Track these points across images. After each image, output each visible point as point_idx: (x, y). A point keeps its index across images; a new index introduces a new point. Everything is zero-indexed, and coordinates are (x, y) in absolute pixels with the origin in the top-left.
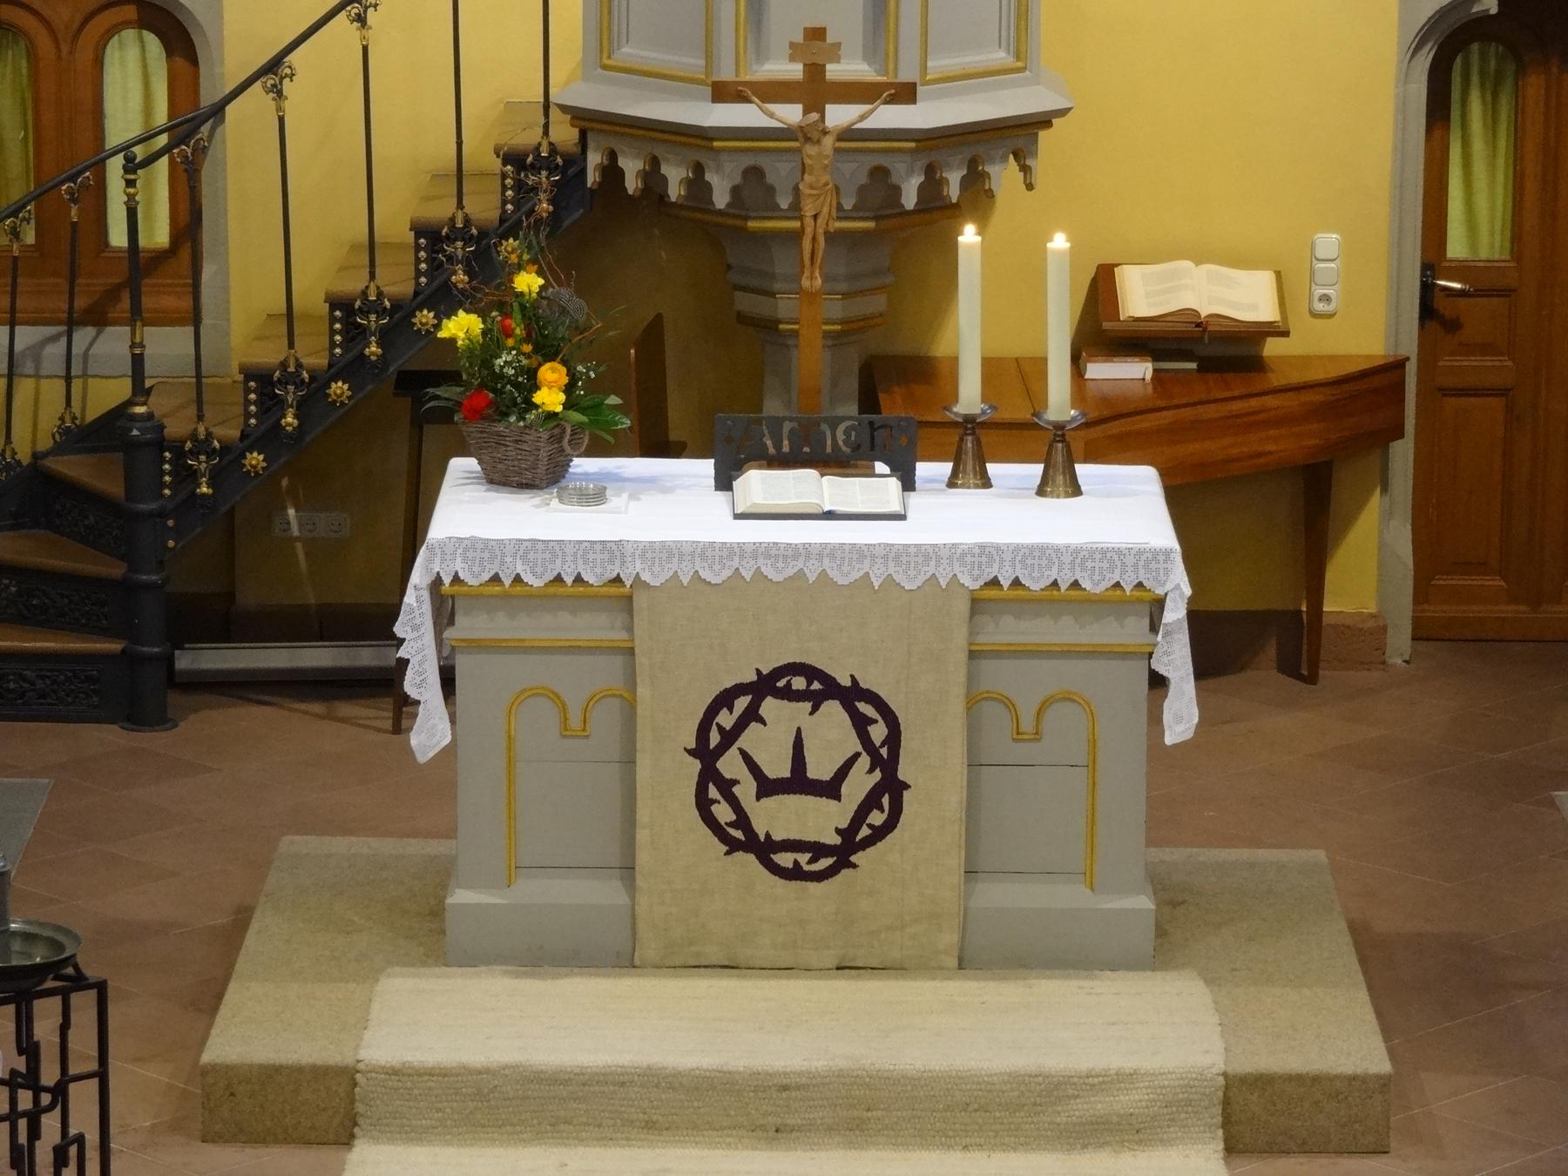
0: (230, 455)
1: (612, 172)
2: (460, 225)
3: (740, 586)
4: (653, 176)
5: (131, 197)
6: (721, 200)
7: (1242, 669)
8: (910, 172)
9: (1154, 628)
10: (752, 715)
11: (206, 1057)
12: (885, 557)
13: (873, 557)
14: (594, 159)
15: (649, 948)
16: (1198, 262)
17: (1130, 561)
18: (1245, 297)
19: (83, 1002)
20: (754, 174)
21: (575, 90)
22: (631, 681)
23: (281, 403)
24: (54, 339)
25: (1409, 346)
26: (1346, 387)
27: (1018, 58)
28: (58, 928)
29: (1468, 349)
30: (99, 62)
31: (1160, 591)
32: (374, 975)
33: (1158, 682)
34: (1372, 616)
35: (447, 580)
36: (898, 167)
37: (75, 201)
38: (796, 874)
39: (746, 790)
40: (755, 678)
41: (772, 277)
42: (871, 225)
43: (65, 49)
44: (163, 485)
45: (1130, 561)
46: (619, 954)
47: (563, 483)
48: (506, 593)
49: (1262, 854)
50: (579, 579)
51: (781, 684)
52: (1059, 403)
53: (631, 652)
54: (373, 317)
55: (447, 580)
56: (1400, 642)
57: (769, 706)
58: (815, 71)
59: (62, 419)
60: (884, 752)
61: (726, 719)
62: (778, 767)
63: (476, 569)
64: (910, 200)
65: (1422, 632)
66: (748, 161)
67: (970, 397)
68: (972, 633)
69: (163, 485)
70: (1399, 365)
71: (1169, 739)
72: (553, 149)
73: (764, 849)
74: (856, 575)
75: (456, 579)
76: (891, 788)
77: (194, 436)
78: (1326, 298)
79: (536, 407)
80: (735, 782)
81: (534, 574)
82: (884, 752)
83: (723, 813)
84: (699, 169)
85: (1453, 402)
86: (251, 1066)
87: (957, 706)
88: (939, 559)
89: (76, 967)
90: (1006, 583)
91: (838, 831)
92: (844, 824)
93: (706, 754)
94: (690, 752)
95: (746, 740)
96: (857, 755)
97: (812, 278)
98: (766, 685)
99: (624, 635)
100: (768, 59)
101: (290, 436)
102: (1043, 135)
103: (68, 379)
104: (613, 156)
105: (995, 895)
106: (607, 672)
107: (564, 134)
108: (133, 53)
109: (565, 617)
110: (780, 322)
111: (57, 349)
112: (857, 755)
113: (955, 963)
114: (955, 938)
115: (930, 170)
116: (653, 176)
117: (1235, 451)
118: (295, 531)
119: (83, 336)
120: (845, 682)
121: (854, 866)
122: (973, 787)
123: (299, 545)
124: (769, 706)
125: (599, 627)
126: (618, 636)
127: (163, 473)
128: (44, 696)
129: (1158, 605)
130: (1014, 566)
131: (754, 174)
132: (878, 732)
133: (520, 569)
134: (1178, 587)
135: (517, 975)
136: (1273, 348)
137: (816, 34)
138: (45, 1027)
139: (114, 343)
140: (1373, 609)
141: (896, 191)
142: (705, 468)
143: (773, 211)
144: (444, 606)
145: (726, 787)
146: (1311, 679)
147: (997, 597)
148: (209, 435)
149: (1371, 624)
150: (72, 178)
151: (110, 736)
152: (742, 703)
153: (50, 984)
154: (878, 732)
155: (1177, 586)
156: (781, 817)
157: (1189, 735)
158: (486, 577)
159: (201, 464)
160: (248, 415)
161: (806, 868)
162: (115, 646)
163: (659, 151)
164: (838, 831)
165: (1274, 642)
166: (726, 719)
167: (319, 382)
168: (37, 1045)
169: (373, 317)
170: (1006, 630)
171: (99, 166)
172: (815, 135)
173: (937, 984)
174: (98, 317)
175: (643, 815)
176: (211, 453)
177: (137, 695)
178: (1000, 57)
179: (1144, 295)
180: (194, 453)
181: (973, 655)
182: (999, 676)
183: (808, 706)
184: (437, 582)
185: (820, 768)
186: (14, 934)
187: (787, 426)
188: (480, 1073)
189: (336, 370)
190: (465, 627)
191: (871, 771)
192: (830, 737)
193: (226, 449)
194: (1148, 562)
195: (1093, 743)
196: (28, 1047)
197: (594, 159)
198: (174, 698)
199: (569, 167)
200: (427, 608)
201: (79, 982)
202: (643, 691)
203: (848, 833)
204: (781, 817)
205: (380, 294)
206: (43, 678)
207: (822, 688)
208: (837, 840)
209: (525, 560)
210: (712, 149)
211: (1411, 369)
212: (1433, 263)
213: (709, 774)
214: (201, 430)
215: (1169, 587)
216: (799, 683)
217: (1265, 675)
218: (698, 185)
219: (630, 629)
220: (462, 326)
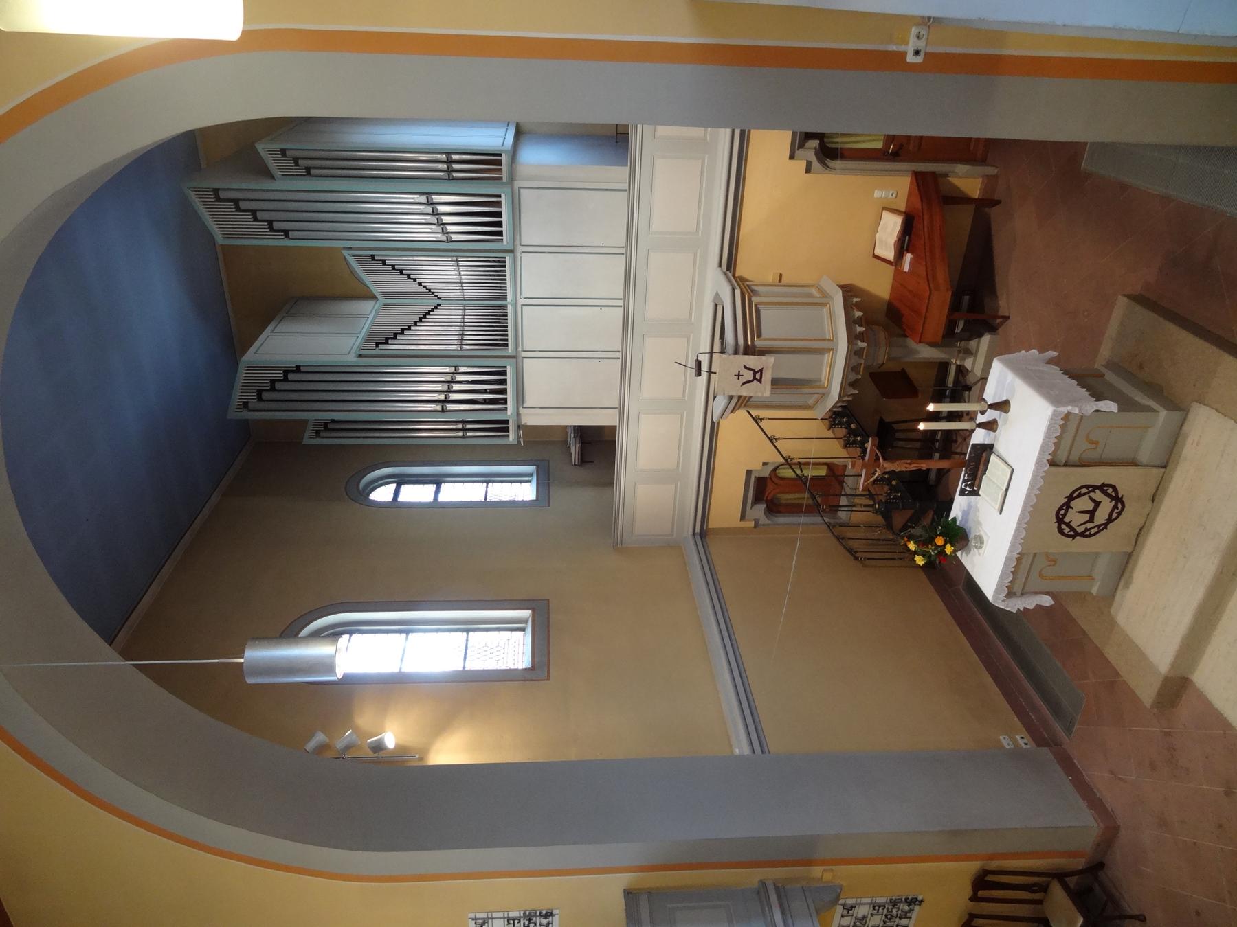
10: (1068, 525)
11: (1148, 706)
18: (891, 226)
36: (856, 348)
39: (1089, 525)
47: (971, 536)
56: (991, 171)
61: (1067, 530)
73: (1110, 520)
98: (1060, 521)
132: (1084, 491)
144: (1011, 594)
145: (1087, 530)
154: (1084, 491)
156: (1101, 516)
174: (841, 483)
185: (1091, 506)
203: (1112, 498)
204: (1101, 516)
207: (1067, 506)
213: (1082, 535)
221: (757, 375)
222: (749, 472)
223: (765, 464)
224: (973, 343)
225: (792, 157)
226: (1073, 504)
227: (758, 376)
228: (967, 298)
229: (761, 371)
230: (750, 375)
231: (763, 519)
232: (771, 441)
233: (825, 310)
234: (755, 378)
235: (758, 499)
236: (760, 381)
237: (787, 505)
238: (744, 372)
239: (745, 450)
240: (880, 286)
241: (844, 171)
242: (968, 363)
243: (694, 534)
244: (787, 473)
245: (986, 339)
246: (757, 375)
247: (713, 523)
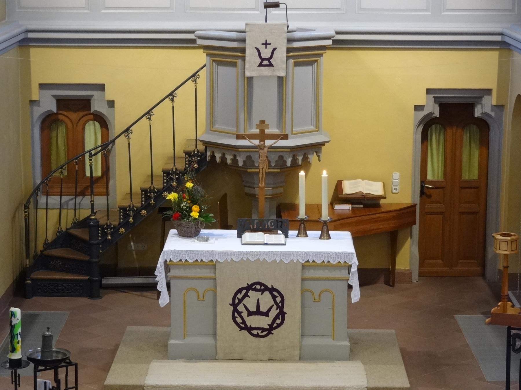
0: (116, 229)
1: (213, 157)
3: (243, 262)
4: (223, 158)
5: (91, 163)
6: (241, 164)
7: (375, 283)
8: (289, 157)
9: (349, 273)
10: (246, 295)
11: (106, 383)
12: (280, 255)
13: (277, 255)
14: (209, 154)
15: (220, 355)
17: (343, 256)
18: (375, 189)
19: (71, 369)
20: (249, 158)
21: (203, 136)
22: (215, 287)
23: (129, 216)
24: (72, 199)
25: (417, 201)
26: (401, 211)
27: (316, 128)
28: (66, 350)
29: (432, 202)
30: (83, 129)
31: (350, 264)
32: (149, 362)
33: (350, 287)
34: (408, 270)
35: (168, 261)
36: (285, 156)
37: (77, 164)
38: (257, 336)
39: (245, 314)
40: (247, 285)
41: (254, 183)
42: (279, 170)
43: (75, 126)
44: (99, 237)
45: (343, 256)
46: (212, 356)
47: (199, 236)
48: (183, 264)
49: (378, 331)
50: (202, 260)
51: (254, 287)
52: (325, 215)
53: (215, 279)
54: (152, 194)
55: (168, 261)
56: (415, 276)
57: (251, 293)
58: (262, 131)
59: (73, 220)
60: (280, 304)
61: (240, 296)
62: (253, 309)
63: (176, 258)
64: (289, 164)
65: (421, 274)
66: (248, 154)
67: (302, 214)
68: (302, 274)
69: (99, 237)
70: (414, 206)
71: (353, 302)
72: (198, 151)
73: (249, 329)
74: (273, 259)
75: (171, 261)
76: (282, 314)
77: (107, 224)
78: (396, 189)
79: (191, 216)
80: (242, 312)
81: (191, 259)
82: (280, 304)
83: (239, 320)
84: (235, 156)
85: (429, 216)
86: (117, 385)
87: (299, 293)
88: (294, 255)
89: (69, 360)
90: (311, 261)
91: (268, 325)
92: (270, 323)
93: (234, 305)
94: (230, 305)
95: (244, 302)
96: (273, 305)
97: (262, 184)
98: (249, 288)
99: (214, 275)
101: (131, 224)
102: (323, 147)
103: (75, 209)
104: (213, 153)
105: (309, 341)
106: (209, 284)
107: (201, 147)
108: (92, 127)
109: (198, 270)
111: (73, 202)
112: (273, 305)
113: (298, 358)
114: (298, 352)
115: (294, 156)
116: (223, 158)
117: (372, 228)
118: (133, 249)
119: (79, 199)
120: (270, 287)
121: (272, 334)
122: (303, 313)
123: (134, 252)
124: (251, 293)
125: (206, 273)
126: (212, 275)
127: (99, 233)
128: (68, 290)
129: (351, 266)
130: (313, 257)
131: (249, 158)
132: (278, 299)
133: (187, 258)
134: (355, 262)
135: (186, 362)
136: (382, 201)
137: (263, 122)
138: (62, 376)
139: (86, 201)
140: (409, 268)
141: (285, 162)
142: (235, 232)
143: (253, 166)
144: (168, 267)
145: (240, 313)
146: (393, 286)
147: (308, 265)
148: (110, 224)
149: (408, 272)
150: (76, 159)
151: (84, 301)
152: (244, 292)
153: (63, 364)
154: (278, 299)
155: (355, 262)
156: (254, 321)
157: (358, 300)
158: (178, 260)
159: (109, 231)
160: (120, 219)
161: (260, 334)
162: (86, 278)
163: (225, 151)
164: (268, 325)
165: (383, 277)
166: (240, 296)
167: (139, 210)
168: (59, 380)
169: (152, 194)
170: (311, 273)
171: (83, 156)
172: (262, 148)
173: (294, 364)
175: (218, 321)
176: (111, 228)
177: (92, 290)
178: (312, 128)
179: (349, 188)
180: (107, 229)
181: (303, 280)
182: (309, 285)
183: (261, 293)
184: (166, 261)
185: (263, 309)
186: (54, 351)
187: (256, 221)
188: (176, 387)
189: (143, 207)
190: (173, 272)
191: (277, 309)
192: (266, 301)
193: (115, 227)
194: (347, 256)
195: (334, 302)
196: (57, 380)
197: (209, 154)
198: (101, 291)
199: (203, 155)
200: (163, 268)
201: (70, 364)
202: (218, 289)
203: (271, 325)
204: (254, 321)
205: (154, 188)
206: (68, 286)
207: (264, 288)
208: (268, 327)
209: (188, 255)
211: (418, 207)
212: (423, 181)
213: (235, 310)
214: (108, 222)
215: (353, 262)
216: (258, 287)
217: (381, 285)
218: (235, 160)
219: (215, 273)
220: (172, 196)
221: (266, 62)
222: (101, 87)
223: (111, 104)
225: (429, 91)
226: (267, 293)
229: (271, 65)
230: (266, 54)
231: (38, 112)
232: (171, 94)
233: (312, 128)
234: (263, 59)
235: (63, 103)
236: (260, 65)
237: (49, 139)
238: (270, 49)
239: (130, 82)
241: (415, 141)
243: (28, 31)
244: (92, 135)
246: (266, 62)
247: (38, 55)
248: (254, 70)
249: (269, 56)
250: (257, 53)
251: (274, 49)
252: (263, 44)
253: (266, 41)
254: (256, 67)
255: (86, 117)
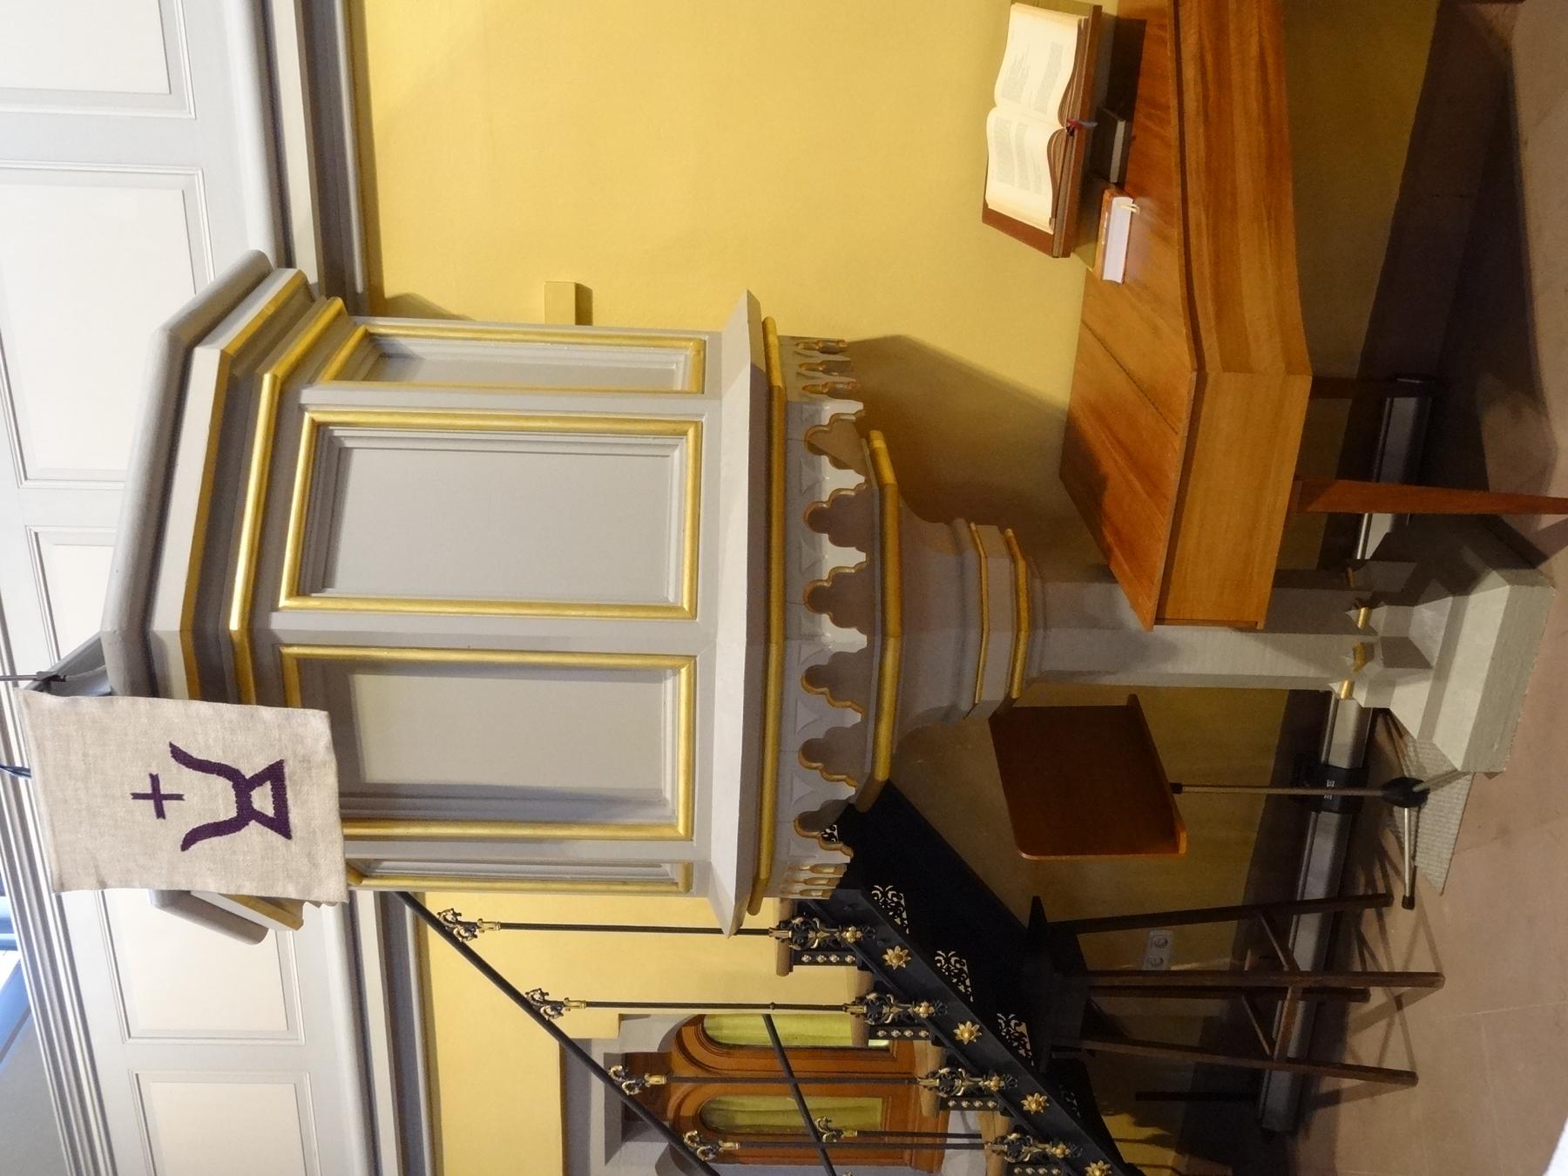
2: (865, 1009)
7: (1507, 51)
8: (813, 637)
16: (992, 104)
30: (730, 1049)
36: (804, 656)
66: (789, 829)
100: (660, 792)
110: (1008, 696)
117: (1254, 107)
165: (1482, 8)
179: (1031, 196)
210: (768, 880)
224: (1428, 618)
227: (262, 800)
228: (1405, 409)
233: (680, 457)
234: (246, 814)
236: (280, 824)
238: (176, 778)
240: (1025, 340)
242: (1407, 702)
245: (1491, 601)
248: (310, 856)
249: (223, 786)
250: (215, 840)
251: (179, 755)
252: (160, 813)
253: (136, 796)
254: (294, 846)
255: (690, 1049)
